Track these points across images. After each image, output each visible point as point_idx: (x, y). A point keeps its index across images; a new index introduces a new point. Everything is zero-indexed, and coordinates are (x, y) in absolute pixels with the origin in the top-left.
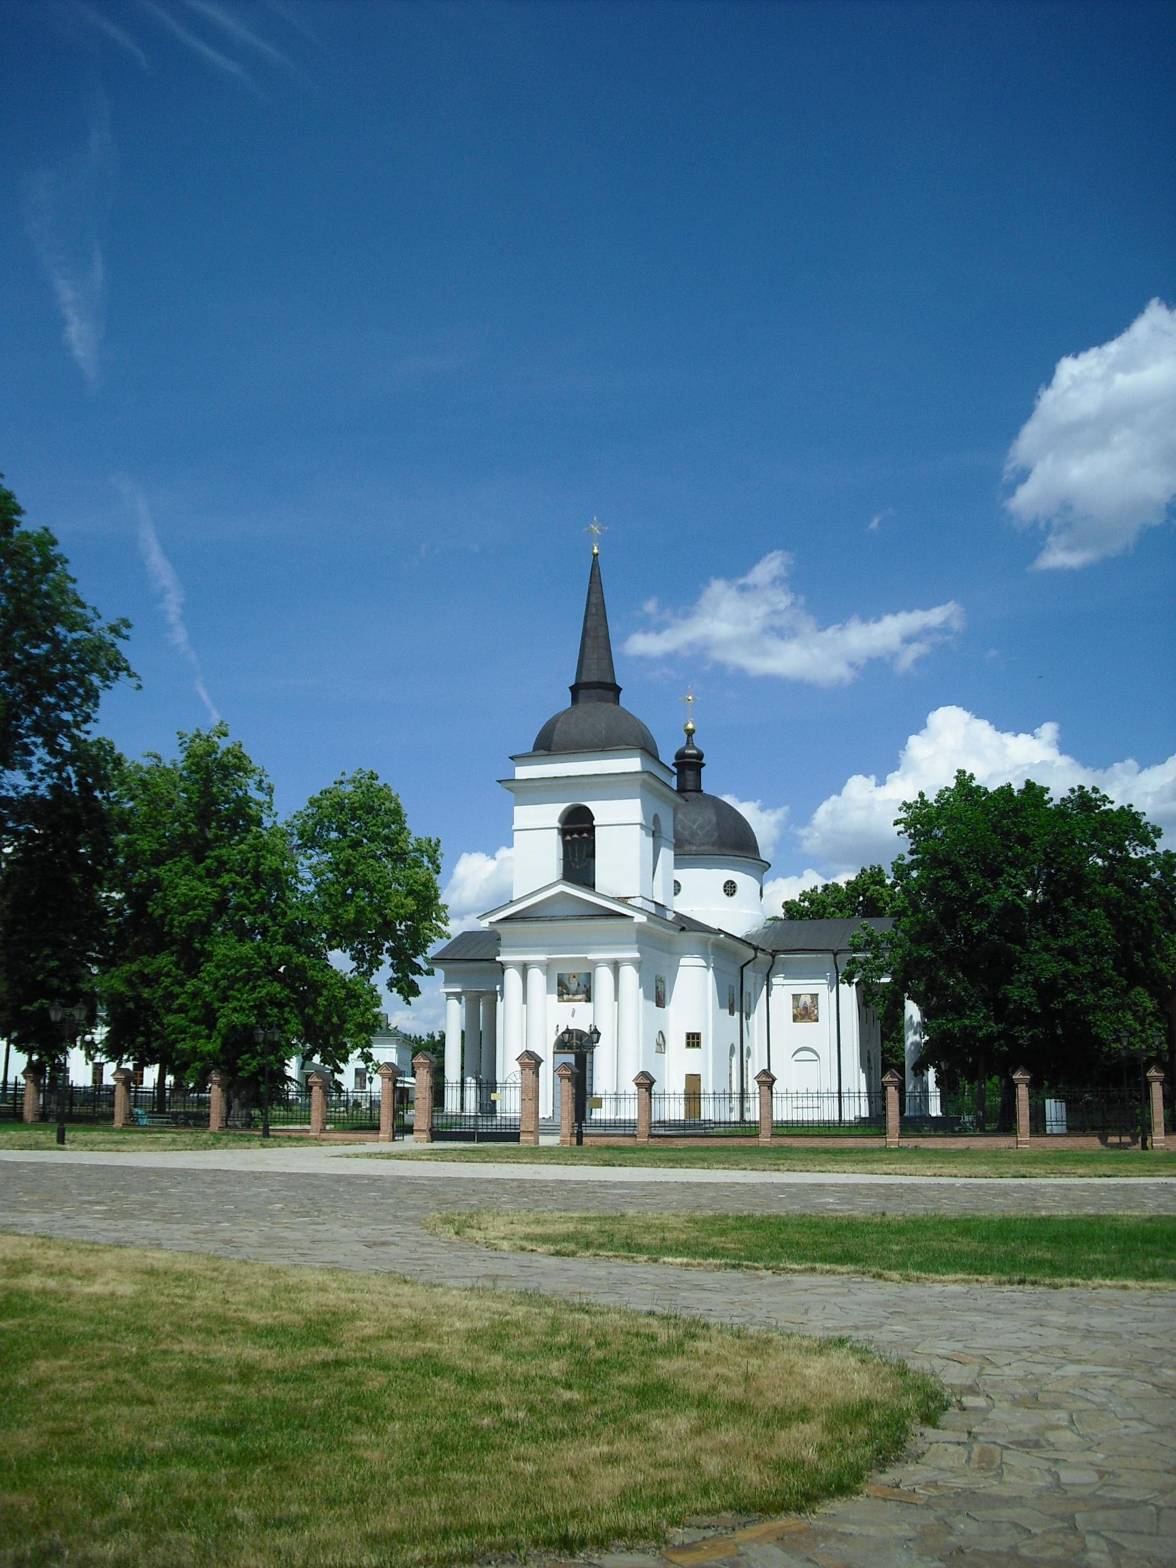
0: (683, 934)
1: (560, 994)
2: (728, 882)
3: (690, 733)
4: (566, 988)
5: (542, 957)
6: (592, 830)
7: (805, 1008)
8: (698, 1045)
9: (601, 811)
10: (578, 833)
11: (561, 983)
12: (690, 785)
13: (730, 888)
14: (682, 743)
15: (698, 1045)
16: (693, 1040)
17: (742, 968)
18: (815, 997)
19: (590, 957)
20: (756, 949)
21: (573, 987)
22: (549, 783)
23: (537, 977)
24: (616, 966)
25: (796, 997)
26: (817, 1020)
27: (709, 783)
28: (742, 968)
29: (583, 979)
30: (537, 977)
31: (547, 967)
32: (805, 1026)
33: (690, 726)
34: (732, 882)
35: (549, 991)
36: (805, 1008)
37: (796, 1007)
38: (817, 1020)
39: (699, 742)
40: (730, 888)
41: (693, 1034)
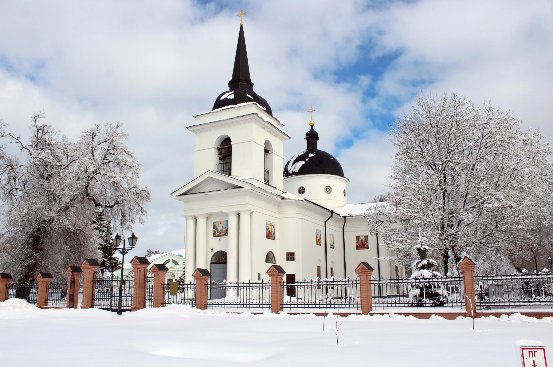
0: (283, 200)
4: (217, 229)
7: (362, 242)
8: (293, 259)
11: (214, 227)
13: (328, 190)
15: (293, 259)
16: (291, 257)
18: (366, 237)
20: (332, 212)
21: (220, 228)
23: (202, 222)
25: (357, 238)
26: (368, 248)
28: (325, 222)
32: (362, 251)
38: (368, 248)
39: (315, 129)
40: (328, 190)
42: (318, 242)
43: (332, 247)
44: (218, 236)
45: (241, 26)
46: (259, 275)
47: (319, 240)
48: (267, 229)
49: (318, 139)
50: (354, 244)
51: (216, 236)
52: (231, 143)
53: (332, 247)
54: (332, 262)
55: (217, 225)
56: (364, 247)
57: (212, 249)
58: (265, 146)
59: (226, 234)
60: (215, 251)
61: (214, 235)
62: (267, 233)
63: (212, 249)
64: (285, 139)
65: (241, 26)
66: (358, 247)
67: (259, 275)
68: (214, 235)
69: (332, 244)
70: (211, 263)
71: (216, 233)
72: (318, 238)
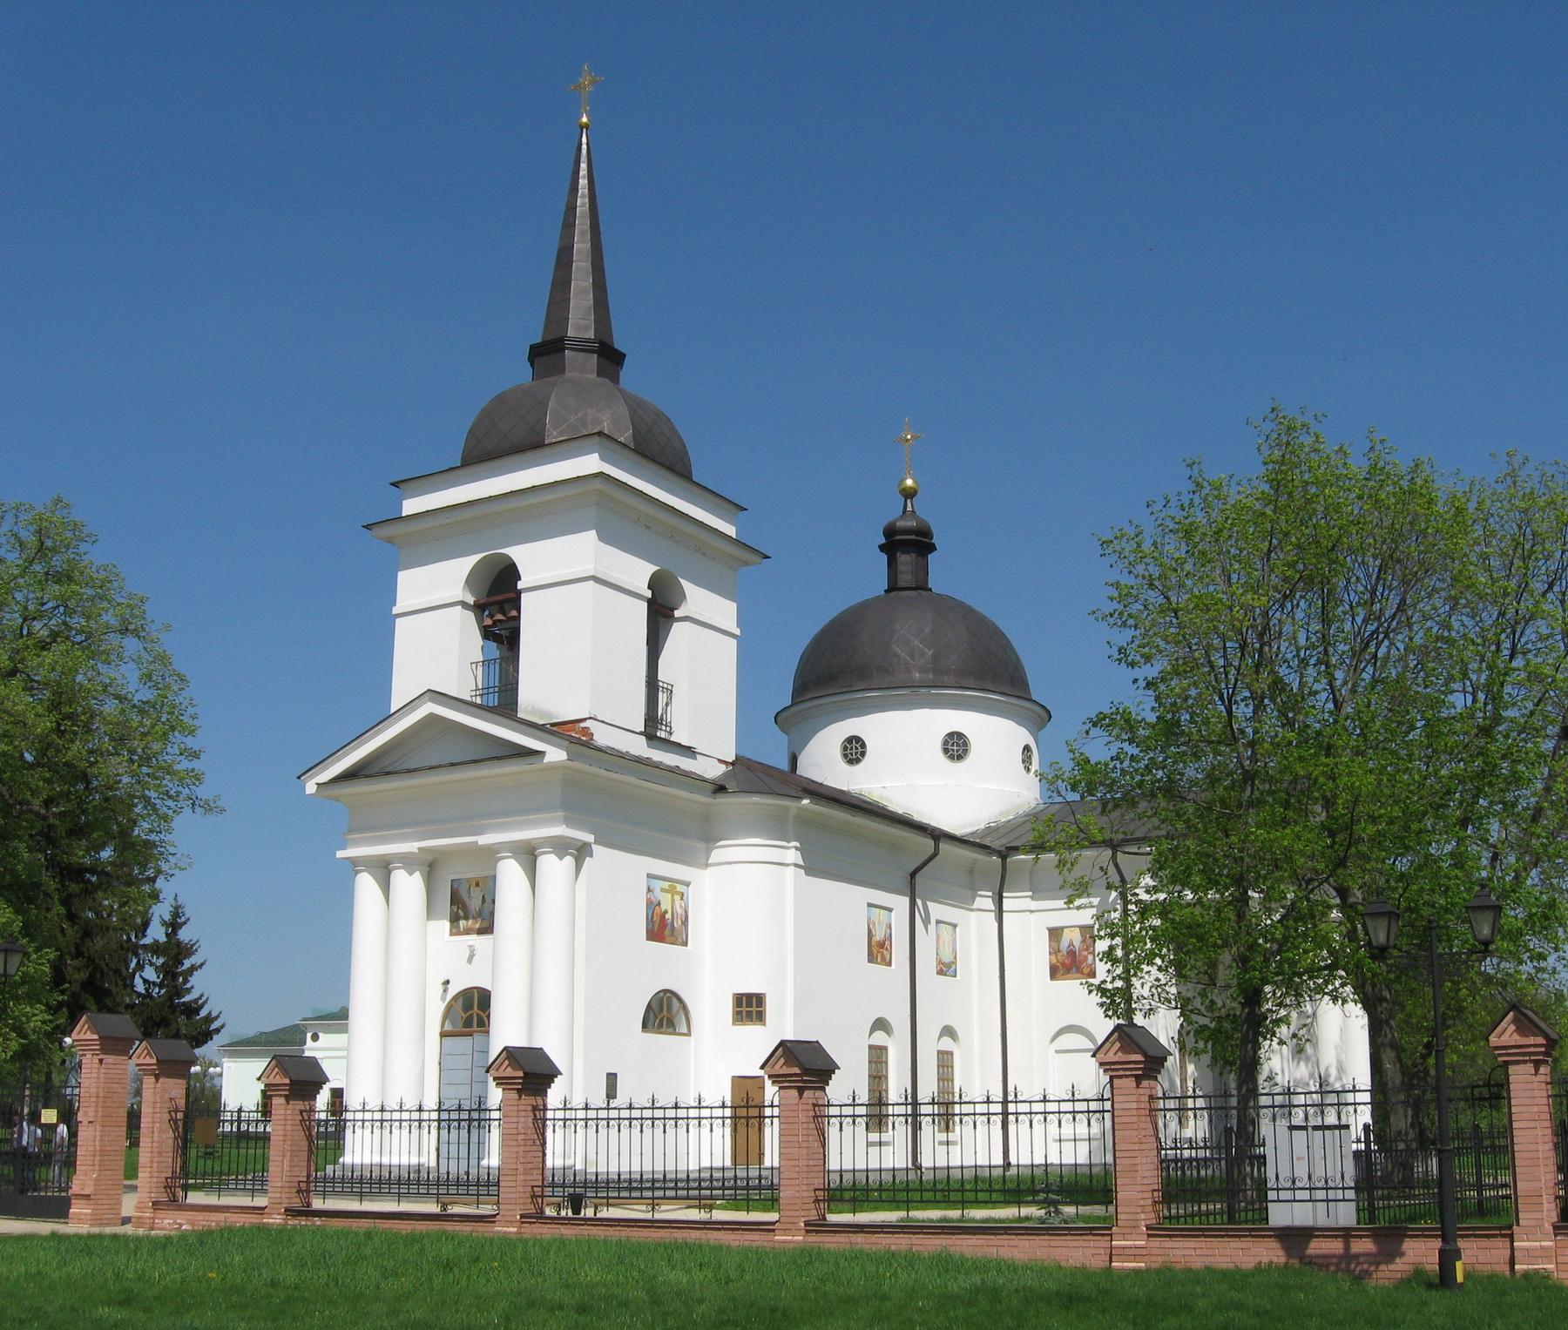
0: (722, 800)
1: (454, 920)
2: (951, 735)
3: (909, 494)
5: (411, 847)
7: (1072, 953)
9: (534, 560)
10: (498, 603)
11: (456, 899)
12: (905, 578)
13: (956, 747)
14: (891, 511)
16: (749, 1007)
17: (913, 875)
19: (484, 840)
22: (442, 520)
27: (943, 574)
28: (913, 875)
30: (409, 885)
31: (430, 866)
33: (909, 482)
34: (960, 735)
35: (431, 912)
36: (1072, 953)
37: (1054, 951)
40: (956, 747)
41: (749, 996)
42: (878, 951)
43: (946, 969)
46: (612, 1079)
47: (882, 945)
48: (652, 905)
49: (932, 548)
50: (933, 966)
51: (459, 933)
52: (520, 585)
53: (946, 969)
54: (948, 1032)
56: (1079, 971)
57: (448, 982)
58: (649, 594)
60: (454, 990)
62: (650, 920)
63: (448, 982)
64: (746, 563)
66: (1055, 973)
67: (612, 1079)
69: (947, 958)
70: (443, 1035)
72: (879, 935)
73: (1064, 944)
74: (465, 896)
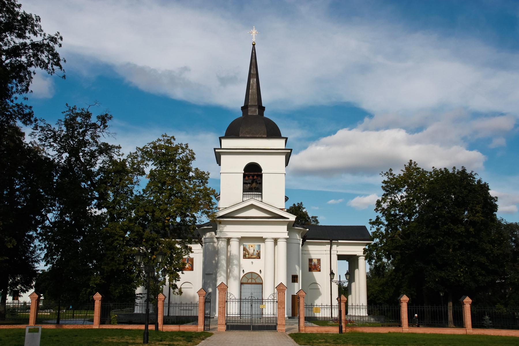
4: (248, 252)
6: (261, 176)
7: (315, 265)
11: (245, 249)
18: (319, 260)
21: (251, 251)
24: (276, 241)
26: (320, 271)
29: (256, 248)
38: (320, 271)
44: (249, 258)
45: (254, 45)
51: (246, 258)
55: (247, 248)
59: (258, 257)
61: (245, 257)
65: (254, 45)
68: (245, 257)
71: (247, 256)
73: (313, 264)
74: (248, 249)
